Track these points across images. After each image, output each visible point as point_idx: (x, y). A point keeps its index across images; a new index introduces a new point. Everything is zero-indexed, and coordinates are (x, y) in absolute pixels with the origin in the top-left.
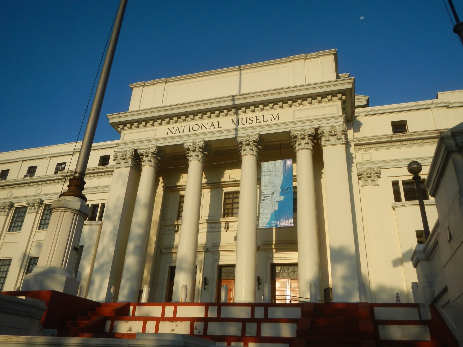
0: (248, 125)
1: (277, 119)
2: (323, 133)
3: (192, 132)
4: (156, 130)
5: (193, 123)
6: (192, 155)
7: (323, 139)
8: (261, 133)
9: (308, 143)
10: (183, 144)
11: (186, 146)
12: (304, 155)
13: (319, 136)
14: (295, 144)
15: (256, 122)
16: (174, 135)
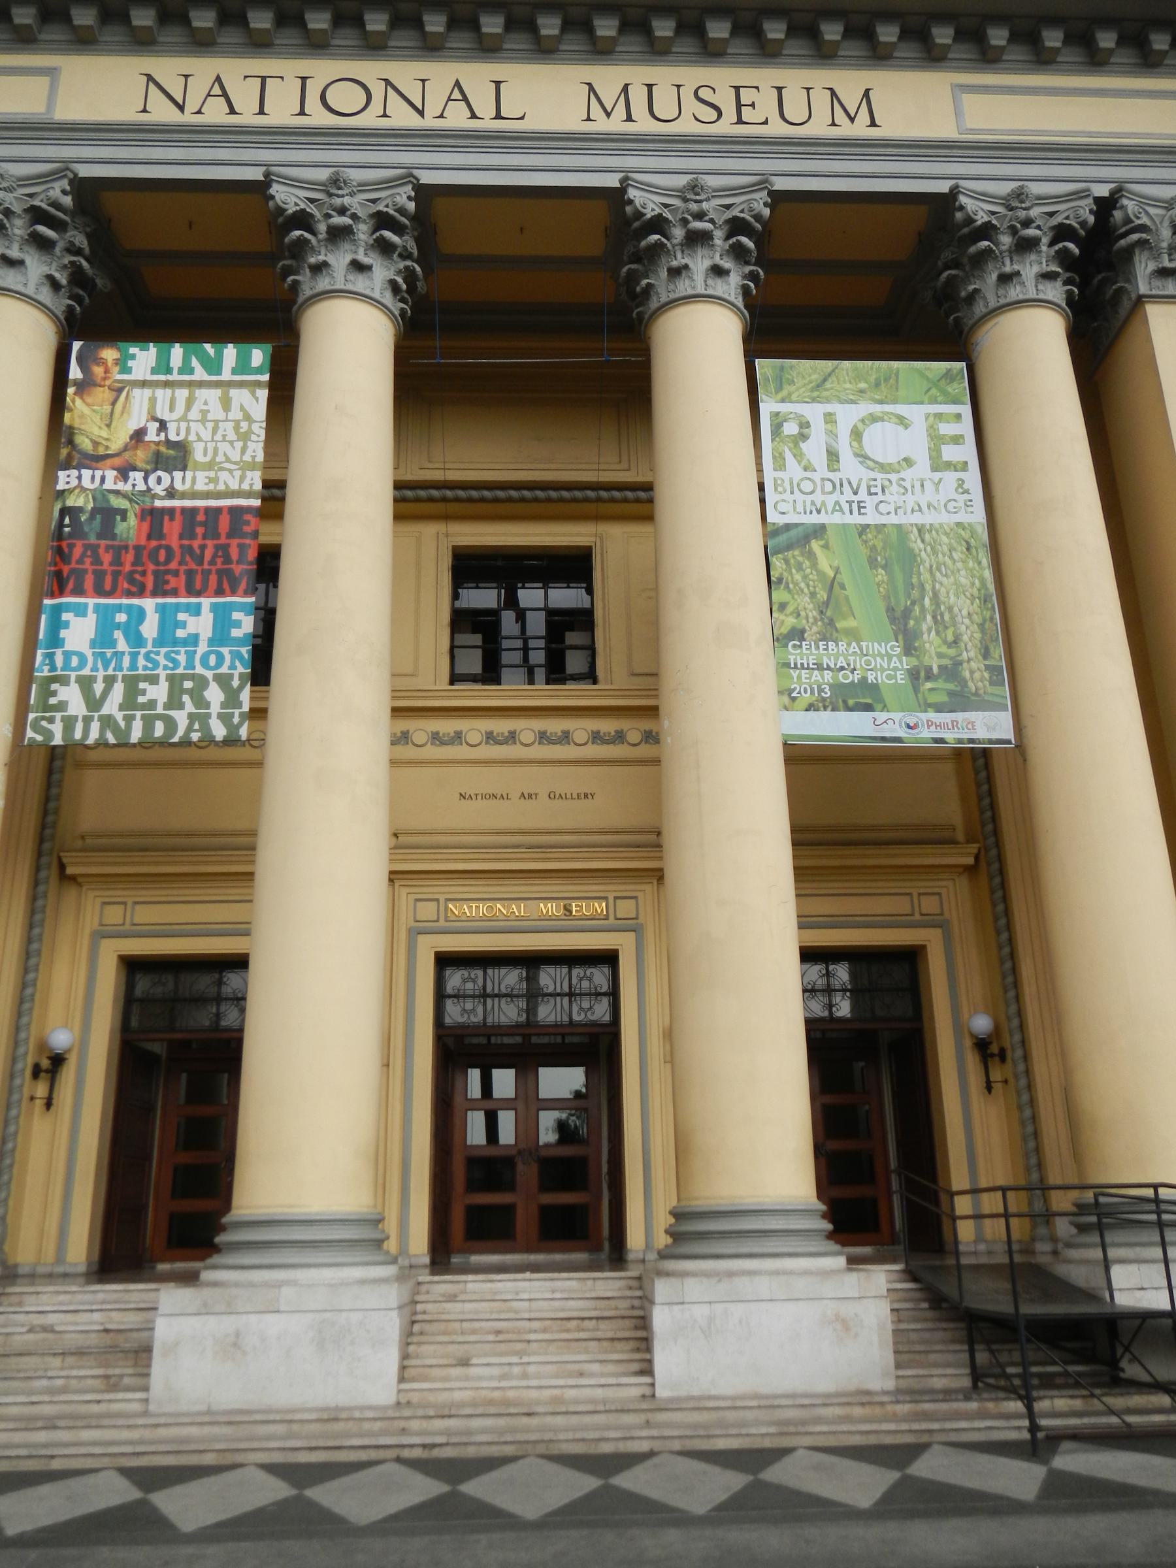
0: (685, 126)
1: (863, 117)
2: (1143, 228)
3: (318, 117)
4: (51, 72)
5: (322, 69)
6: (331, 259)
7: (1144, 267)
8: (781, 184)
9: (1048, 276)
10: (260, 188)
11: (288, 198)
12: (1033, 343)
13: (1123, 242)
14: (966, 280)
15: (740, 121)
16: (188, 118)
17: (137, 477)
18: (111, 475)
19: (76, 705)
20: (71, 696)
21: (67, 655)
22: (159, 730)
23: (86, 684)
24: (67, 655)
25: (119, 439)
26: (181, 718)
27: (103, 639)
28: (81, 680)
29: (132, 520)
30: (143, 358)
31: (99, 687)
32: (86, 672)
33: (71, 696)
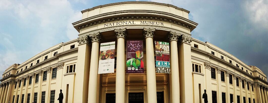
17: (161, 51)
18: (159, 51)
19: (160, 70)
20: (159, 68)
21: (158, 65)
22: (164, 72)
23: (160, 68)
24: (158, 65)
25: (160, 49)
26: (165, 71)
27: (161, 64)
28: (160, 67)
29: (162, 55)
30: (161, 43)
31: (161, 68)
32: (160, 67)
33: (159, 68)
